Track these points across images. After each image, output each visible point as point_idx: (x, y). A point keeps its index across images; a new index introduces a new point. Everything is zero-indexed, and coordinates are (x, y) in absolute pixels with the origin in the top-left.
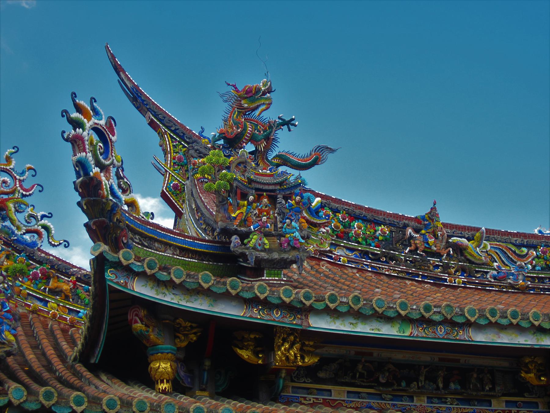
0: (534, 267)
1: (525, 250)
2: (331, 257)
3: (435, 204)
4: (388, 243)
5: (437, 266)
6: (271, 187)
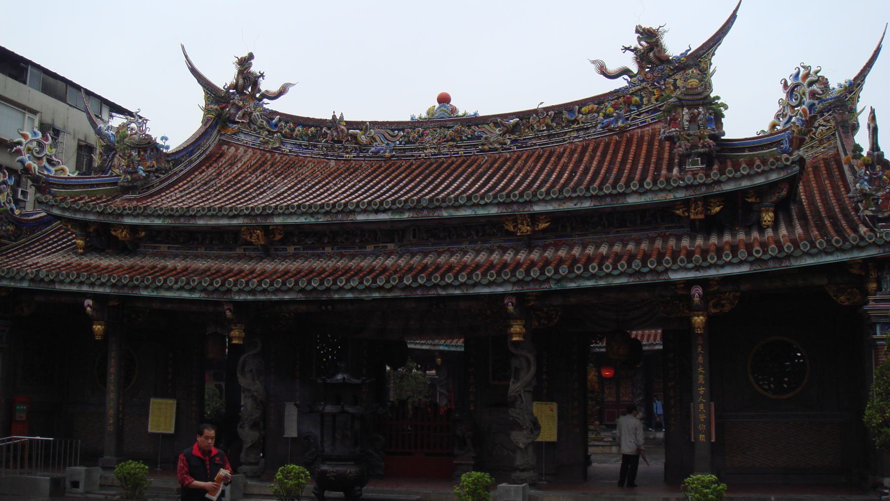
0: (400, 143)
1: (396, 132)
3: (334, 112)
4: (313, 137)
5: (340, 148)
6: (145, 146)
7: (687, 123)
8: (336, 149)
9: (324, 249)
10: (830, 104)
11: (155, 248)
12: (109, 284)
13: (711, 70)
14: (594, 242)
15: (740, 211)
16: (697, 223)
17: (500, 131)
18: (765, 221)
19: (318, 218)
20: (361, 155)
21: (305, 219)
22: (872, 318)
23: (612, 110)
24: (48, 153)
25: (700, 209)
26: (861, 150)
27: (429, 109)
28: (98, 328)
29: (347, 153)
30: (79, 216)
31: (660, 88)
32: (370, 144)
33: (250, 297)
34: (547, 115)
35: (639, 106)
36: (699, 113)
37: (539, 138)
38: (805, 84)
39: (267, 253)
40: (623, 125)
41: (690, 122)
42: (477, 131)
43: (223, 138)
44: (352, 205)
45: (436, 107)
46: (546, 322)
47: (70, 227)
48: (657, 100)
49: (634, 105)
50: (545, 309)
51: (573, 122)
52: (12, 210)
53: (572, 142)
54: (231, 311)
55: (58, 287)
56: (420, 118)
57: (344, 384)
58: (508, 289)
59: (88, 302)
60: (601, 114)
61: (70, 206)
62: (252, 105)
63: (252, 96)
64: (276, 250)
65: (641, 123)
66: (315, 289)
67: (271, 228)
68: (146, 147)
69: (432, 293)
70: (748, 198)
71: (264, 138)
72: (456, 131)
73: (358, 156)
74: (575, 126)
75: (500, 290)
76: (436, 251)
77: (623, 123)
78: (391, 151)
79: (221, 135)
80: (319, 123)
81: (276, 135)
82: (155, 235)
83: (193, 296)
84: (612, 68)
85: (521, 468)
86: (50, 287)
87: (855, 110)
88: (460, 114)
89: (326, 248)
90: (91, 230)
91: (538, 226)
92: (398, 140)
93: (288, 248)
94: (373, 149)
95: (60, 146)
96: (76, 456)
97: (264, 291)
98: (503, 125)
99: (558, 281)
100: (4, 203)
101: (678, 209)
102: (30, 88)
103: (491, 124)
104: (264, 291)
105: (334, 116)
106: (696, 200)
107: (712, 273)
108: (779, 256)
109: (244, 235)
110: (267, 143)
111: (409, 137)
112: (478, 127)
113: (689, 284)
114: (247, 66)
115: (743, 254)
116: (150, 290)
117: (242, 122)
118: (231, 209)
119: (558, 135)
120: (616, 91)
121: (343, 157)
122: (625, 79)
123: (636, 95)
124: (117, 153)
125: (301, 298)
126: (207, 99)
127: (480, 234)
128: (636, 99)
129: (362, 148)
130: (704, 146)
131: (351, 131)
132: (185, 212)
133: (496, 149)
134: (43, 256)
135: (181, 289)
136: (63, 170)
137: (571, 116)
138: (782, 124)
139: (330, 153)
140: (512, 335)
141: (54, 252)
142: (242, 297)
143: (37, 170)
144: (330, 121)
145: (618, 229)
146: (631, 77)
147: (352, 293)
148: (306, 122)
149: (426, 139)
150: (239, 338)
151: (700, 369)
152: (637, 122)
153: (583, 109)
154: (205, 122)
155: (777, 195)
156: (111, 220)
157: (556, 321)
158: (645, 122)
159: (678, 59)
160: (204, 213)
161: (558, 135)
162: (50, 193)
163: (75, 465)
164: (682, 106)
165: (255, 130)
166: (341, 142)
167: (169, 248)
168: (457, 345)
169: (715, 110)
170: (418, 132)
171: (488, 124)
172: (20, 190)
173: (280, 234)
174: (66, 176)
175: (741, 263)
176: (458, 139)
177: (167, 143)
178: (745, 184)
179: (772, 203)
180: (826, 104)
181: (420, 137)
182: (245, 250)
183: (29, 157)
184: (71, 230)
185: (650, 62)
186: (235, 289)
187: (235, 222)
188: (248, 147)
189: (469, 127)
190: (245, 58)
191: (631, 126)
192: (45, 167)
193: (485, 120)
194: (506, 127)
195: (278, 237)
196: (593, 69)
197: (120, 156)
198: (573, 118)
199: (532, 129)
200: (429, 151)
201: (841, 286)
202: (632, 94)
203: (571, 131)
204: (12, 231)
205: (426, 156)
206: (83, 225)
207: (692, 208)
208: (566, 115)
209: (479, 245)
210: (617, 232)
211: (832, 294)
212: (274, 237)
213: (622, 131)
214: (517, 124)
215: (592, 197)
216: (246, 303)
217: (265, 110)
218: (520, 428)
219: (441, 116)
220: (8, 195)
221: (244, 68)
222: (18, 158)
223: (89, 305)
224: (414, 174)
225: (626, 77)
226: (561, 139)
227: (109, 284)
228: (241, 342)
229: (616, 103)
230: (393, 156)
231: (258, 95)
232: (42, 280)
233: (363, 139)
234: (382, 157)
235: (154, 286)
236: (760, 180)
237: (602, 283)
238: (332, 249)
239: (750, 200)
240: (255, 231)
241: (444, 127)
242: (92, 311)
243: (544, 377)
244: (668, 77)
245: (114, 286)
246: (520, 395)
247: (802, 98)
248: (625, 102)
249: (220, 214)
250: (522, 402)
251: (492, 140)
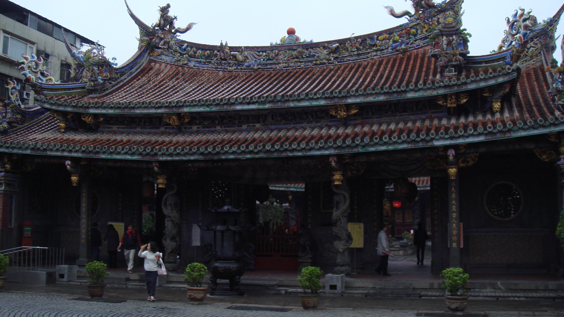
0: (264, 60)
1: (261, 53)
2: (188, 65)
3: (221, 41)
4: (208, 57)
5: (226, 64)
6: (102, 64)
7: (446, 46)
8: (223, 64)
9: (215, 128)
10: (538, 33)
11: (109, 128)
12: (80, 151)
13: (461, 12)
14: (386, 122)
15: (479, 102)
16: (452, 110)
17: (327, 52)
18: (495, 108)
19: (211, 108)
20: (239, 68)
21: (204, 109)
22: (563, 169)
23: (398, 38)
24: (41, 69)
25: (454, 100)
26: (556, 62)
27: (282, 38)
28: (74, 178)
29: (230, 66)
30: (61, 109)
31: (429, 23)
32: (245, 61)
33: (169, 158)
34: (357, 41)
35: (415, 35)
36: (453, 39)
37: (352, 56)
38: (521, 20)
39: (180, 130)
40: (405, 47)
41: (447, 45)
42: (312, 52)
43: (151, 58)
44: (233, 99)
45: (286, 37)
46: (356, 173)
47: (56, 115)
48: (426, 31)
49: (412, 35)
50: (355, 165)
51: (373, 46)
52: (19, 105)
53: (373, 59)
54: (157, 167)
55: (49, 153)
56: (276, 44)
57: (228, 212)
58: (332, 151)
59: (68, 162)
60: (391, 40)
61: (55, 102)
62: (169, 37)
63: (170, 31)
64: (185, 128)
65: (417, 46)
66: (210, 153)
67: (182, 114)
68: (103, 65)
69: (284, 155)
70: (484, 93)
71: (177, 58)
72: (299, 52)
73: (237, 69)
74: (375, 48)
75: (327, 152)
76: (286, 128)
77: (405, 46)
78: (258, 65)
79: (151, 56)
80: (212, 48)
81: (185, 56)
82: (110, 120)
83: (133, 158)
84: (398, 11)
85: (341, 264)
86: (44, 153)
87: (554, 37)
88: (302, 41)
89: (217, 127)
90: (69, 117)
91: (351, 112)
92: (262, 58)
93: (193, 127)
94: (246, 64)
95: (50, 64)
96: (62, 258)
97: (178, 154)
98: (329, 48)
99: (364, 147)
100: (14, 101)
101: (440, 101)
102: (29, 28)
103: (321, 48)
104: (178, 154)
105: (222, 43)
106: (451, 95)
107: (461, 141)
108: (504, 130)
109: (165, 119)
110: (179, 61)
111: (269, 56)
112: (313, 50)
113: (446, 148)
114: (166, 12)
115: (480, 129)
116: (106, 155)
117: (164, 48)
118: (157, 103)
119: (364, 54)
120: (401, 26)
121: (227, 69)
122: (407, 18)
123: (414, 28)
124: (85, 68)
125: (201, 158)
126: (141, 33)
127: (314, 117)
128: (413, 30)
129: (239, 63)
130: (456, 61)
131: (232, 53)
132: (128, 105)
133: (324, 63)
134: (39, 134)
135: (126, 153)
136: (51, 79)
137: (372, 42)
138: (506, 46)
139: (219, 67)
140: (334, 181)
141: (46, 131)
142: (164, 158)
143: (34, 80)
144: (219, 47)
145: (401, 114)
146: (410, 17)
147: (234, 155)
148: (204, 48)
149: (280, 57)
150: (162, 184)
151: (453, 202)
152: (414, 45)
153: (380, 38)
154: (140, 48)
155: (503, 91)
156: (81, 111)
157: (362, 172)
158: (419, 45)
159: (440, 5)
160: (139, 106)
161: (364, 54)
162: (43, 94)
163: (62, 264)
164: (442, 35)
165: (171, 53)
166: (225, 59)
167: (118, 128)
168: (300, 187)
169: (463, 37)
170: (275, 53)
171: (319, 47)
172: (25, 92)
173: (188, 118)
174: (53, 83)
175: (479, 134)
176: (300, 57)
177: (116, 62)
178: (482, 84)
179: (500, 96)
180: (535, 33)
181: (276, 56)
182: (166, 128)
183: (29, 72)
184: (56, 117)
185: (422, 7)
186: (160, 153)
187: (159, 111)
188: (168, 64)
189: (307, 49)
190: (165, 7)
191: (410, 48)
192: (39, 78)
193: (318, 45)
194: (331, 49)
195: (187, 120)
196: (386, 12)
197: (87, 70)
198: (373, 43)
199: (347, 51)
200: (282, 65)
201: (544, 149)
202: (411, 28)
203: (372, 52)
204: (19, 118)
205: (280, 68)
206: (64, 114)
207: (449, 100)
208: (369, 41)
209: (313, 125)
210: (402, 115)
211: (537, 155)
212: (184, 120)
213: (404, 51)
214: (338, 47)
215: (385, 93)
216: (166, 162)
217: (178, 40)
218: (340, 239)
219: (289, 43)
220: (17, 96)
221: (164, 13)
222: (22, 73)
223: (68, 165)
224: (272, 79)
225: (407, 16)
226: (365, 56)
227: (80, 151)
228: (164, 187)
229: (401, 34)
230: (259, 68)
231: (173, 31)
232: (39, 149)
233: (240, 58)
234: (252, 69)
235: (109, 152)
236: (492, 82)
237: (391, 148)
238: (221, 127)
239: (485, 95)
240: (172, 117)
241: (292, 50)
242: (71, 168)
243: (355, 207)
244: (434, 17)
245: (84, 152)
246: (340, 219)
247: (519, 30)
248: (406, 33)
249: (150, 106)
250: (341, 223)
251: (322, 58)
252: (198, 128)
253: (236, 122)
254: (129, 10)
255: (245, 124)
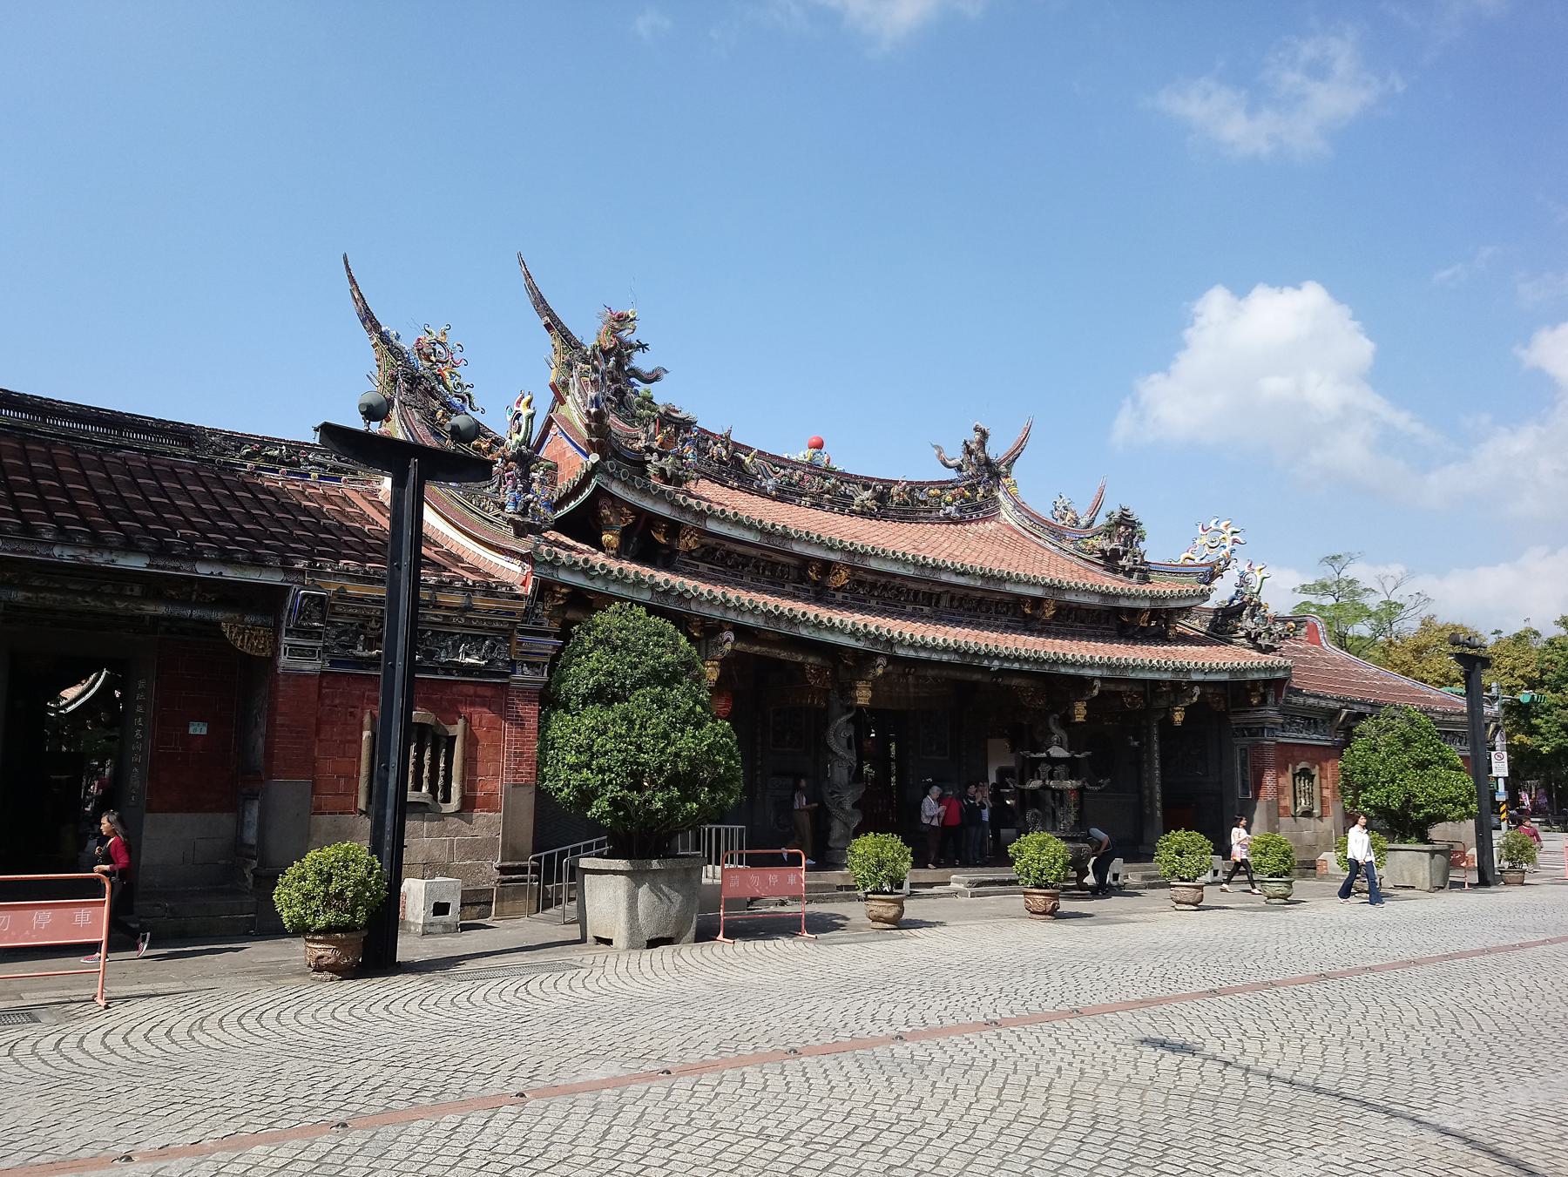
0: (782, 482)
84: (947, 455)
103: (860, 486)
124: (420, 384)
171: (857, 484)
203: (920, 511)
238: (877, 603)
240: (841, 571)
252: (844, 597)
253: (902, 599)
254: (532, 289)
255: (911, 603)
